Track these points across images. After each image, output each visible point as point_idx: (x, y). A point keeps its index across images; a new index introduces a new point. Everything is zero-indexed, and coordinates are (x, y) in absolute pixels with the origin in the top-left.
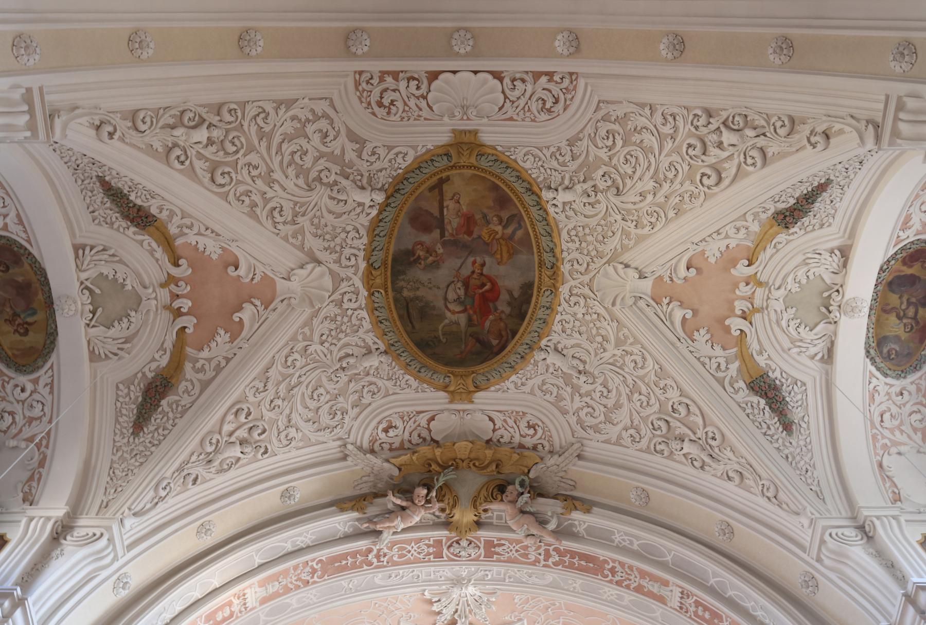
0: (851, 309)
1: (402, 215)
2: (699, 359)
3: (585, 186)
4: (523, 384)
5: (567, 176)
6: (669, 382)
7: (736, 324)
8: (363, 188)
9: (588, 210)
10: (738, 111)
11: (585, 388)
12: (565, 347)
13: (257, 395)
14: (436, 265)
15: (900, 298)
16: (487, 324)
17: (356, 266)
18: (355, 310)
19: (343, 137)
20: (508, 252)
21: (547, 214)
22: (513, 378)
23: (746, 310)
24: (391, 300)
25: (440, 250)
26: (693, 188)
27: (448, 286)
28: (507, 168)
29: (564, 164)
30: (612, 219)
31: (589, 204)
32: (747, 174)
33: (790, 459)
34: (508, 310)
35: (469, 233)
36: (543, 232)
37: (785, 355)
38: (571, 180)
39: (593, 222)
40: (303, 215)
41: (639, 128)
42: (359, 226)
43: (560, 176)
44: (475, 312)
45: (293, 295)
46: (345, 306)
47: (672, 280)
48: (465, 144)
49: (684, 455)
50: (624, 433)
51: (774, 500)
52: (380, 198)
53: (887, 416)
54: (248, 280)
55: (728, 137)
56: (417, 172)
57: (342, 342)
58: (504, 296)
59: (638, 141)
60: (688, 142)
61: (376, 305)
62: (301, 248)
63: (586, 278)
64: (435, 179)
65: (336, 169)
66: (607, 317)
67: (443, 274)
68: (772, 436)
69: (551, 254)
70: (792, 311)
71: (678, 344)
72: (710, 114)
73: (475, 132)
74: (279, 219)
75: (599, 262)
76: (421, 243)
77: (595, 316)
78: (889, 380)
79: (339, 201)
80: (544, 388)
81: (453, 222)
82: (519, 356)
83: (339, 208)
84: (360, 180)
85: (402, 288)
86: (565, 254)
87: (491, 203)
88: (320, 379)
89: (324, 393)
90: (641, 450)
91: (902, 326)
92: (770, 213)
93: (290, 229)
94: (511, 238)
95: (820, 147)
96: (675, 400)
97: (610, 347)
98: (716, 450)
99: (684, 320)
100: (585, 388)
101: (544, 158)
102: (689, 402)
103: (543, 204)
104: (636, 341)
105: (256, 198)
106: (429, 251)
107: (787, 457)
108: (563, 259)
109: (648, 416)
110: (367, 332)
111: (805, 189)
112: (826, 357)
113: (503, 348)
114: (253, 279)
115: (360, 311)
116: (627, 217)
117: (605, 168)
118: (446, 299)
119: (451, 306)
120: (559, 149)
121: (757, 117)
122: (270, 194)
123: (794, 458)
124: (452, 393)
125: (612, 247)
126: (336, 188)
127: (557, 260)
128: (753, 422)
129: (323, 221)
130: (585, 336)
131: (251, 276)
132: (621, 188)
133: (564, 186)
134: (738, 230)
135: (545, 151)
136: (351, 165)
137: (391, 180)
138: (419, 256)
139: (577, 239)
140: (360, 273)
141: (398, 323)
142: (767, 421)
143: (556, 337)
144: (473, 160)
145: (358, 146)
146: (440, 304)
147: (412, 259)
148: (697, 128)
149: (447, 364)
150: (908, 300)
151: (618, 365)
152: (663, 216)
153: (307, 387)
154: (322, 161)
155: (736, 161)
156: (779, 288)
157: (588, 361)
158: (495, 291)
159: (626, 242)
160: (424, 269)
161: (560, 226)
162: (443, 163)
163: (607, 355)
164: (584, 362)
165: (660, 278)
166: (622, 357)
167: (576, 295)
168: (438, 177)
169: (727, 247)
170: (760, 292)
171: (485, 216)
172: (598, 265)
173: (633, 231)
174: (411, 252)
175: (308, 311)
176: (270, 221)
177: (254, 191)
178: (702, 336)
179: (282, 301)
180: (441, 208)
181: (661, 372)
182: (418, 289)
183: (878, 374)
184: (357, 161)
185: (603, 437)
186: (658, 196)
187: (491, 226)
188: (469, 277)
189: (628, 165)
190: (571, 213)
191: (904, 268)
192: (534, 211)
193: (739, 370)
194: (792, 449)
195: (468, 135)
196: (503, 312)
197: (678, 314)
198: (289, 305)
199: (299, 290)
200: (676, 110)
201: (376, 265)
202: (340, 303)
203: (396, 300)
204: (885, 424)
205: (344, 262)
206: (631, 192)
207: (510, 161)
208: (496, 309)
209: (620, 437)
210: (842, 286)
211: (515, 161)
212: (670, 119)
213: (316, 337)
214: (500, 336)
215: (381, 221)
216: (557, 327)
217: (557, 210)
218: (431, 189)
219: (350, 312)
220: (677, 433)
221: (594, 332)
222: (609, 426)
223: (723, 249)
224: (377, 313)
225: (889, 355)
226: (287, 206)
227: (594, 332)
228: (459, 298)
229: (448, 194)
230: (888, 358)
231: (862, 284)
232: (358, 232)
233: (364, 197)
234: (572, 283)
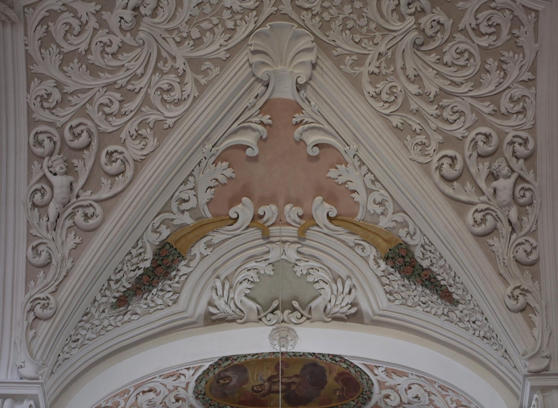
0: (283, 332)
2: (191, 175)
6: (152, 143)
7: (244, 210)
10: (537, 194)
11: (112, 19)
15: (296, 376)
23: (265, 219)
26: (434, 146)
30: (378, 39)
32: (461, 215)
33: (85, 318)
37: (209, 272)
41: (504, 66)
47: (298, 124)
49: (45, 176)
50: (51, 83)
51: (32, 316)
53: (151, 395)
55: (504, 185)
59: (487, 67)
60: (494, 134)
68: (109, 288)
70: (269, 271)
71: (209, 146)
72: (529, 158)
77: (230, 25)
78: (192, 385)
90: (30, 111)
91: (261, 382)
92: (408, 240)
95: (511, 303)
96: (126, 154)
98: (69, 223)
99: (244, 147)
100: (112, 19)
102: (129, 173)
104: (202, 89)
107: (86, 314)
109: (88, 116)
111: (444, 279)
112: (214, 318)
116: (383, 59)
117: (449, 23)
121: (532, 218)
123: (87, 322)
125: (338, 42)
128: (122, 262)
130: (196, 12)
132: (423, 48)
134: (381, 204)
142: (125, 277)
148: (512, 143)
150: (294, 383)
151: (160, 65)
152: (392, 109)
155: (475, 199)
156: (299, 252)
157: (157, 20)
159: (348, 60)
164: (154, 15)
165: (300, 109)
166: (174, 70)
169: (354, 191)
170: (291, 232)
172: (309, 24)
173: (365, 70)
178: (223, 172)
181: (162, 130)
183: (200, 372)
185: (37, 56)
186: (417, 99)
189: (456, 56)
191: (335, 374)
193: (182, 226)
194: (96, 315)
197: (248, 139)
200: (530, 113)
204: (141, 398)
206: (419, 63)
209: (42, 77)
210: (308, 319)
212: (518, 108)
220: (75, 161)
221: (206, 25)
222: (57, 59)
223: (351, 186)
225: (222, 378)
230: (219, 378)
231: (314, 340)
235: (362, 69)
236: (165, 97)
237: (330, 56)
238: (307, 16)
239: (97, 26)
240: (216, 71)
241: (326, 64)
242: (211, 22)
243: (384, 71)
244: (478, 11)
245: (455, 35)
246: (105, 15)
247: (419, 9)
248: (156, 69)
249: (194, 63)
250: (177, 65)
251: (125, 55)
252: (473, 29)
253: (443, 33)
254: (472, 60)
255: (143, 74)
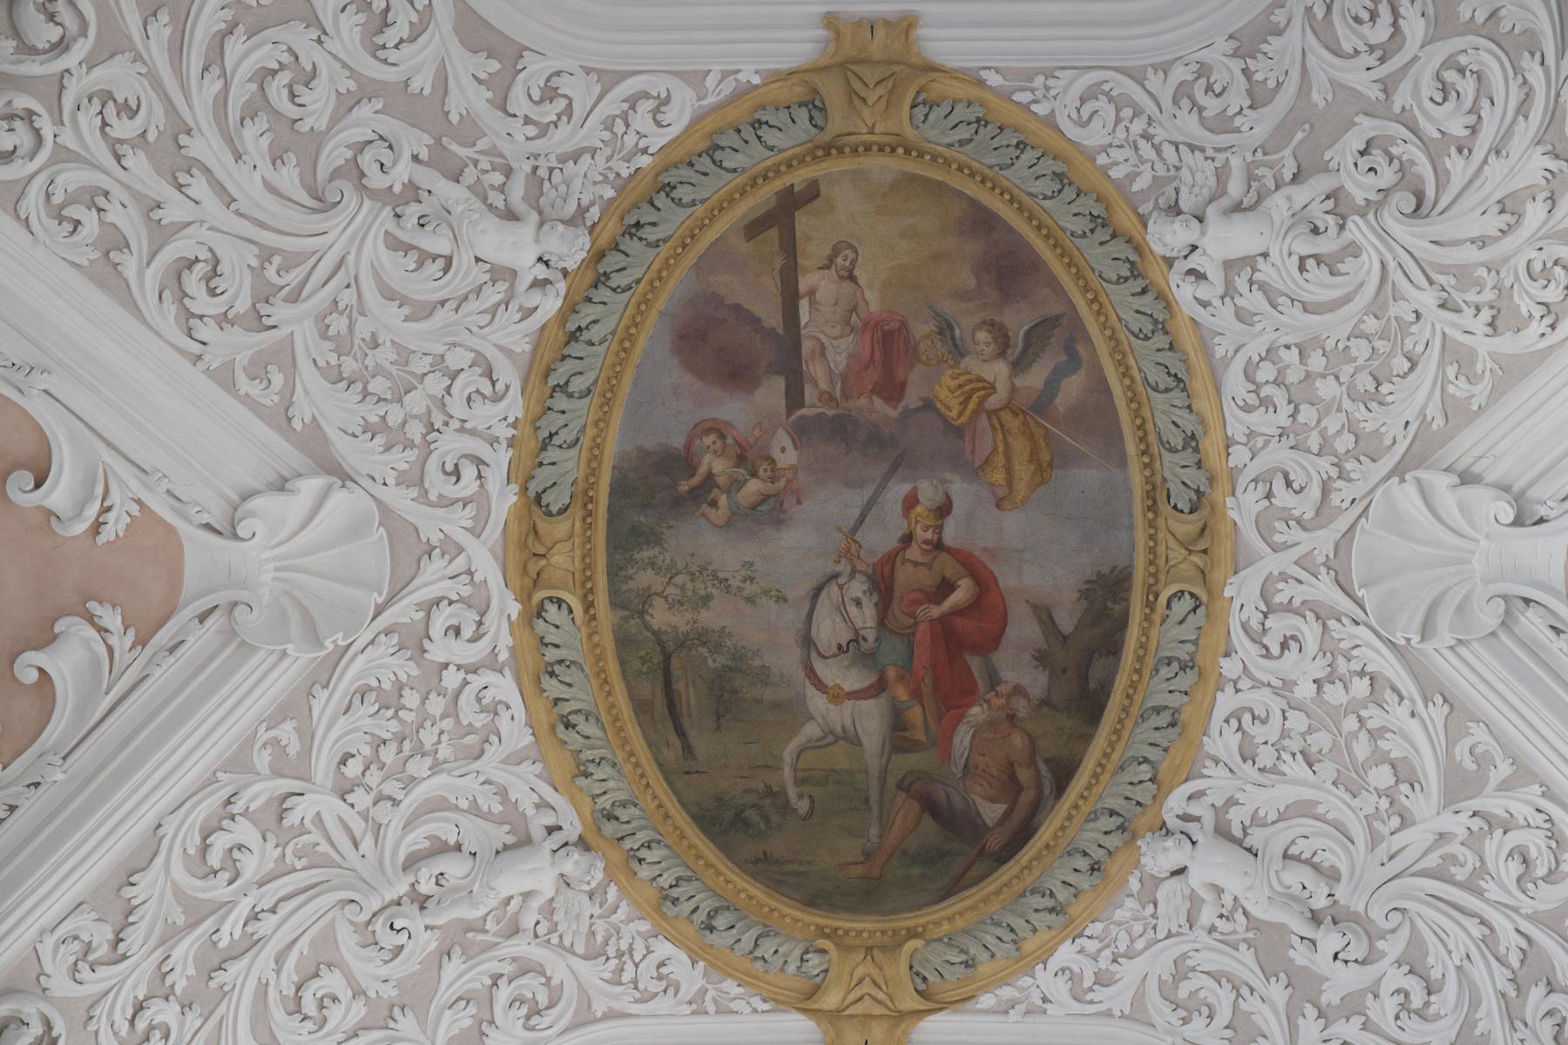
1: (653, 316)
3: (1301, 195)
4: (1103, 980)
5: (1236, 163)
8: (511, 216)
9: (1319, 285)
11: (1341, 982)
12: (1257, 820)
13: (85, 973)
14: (771, 512)
16: (962, 739)
17: (480, 500)
18: (474, 670)
19: (442, 37)
20: (1034, 457)
21: (1168, 307)
22: (1065, 954)
24: (607, 640)
25: (787, 456)
27: (817, 592)
28: (1021, 146)
29: (1222, 124)
30: (1403, 310)
31: (1319, 259)
34: (1036, 682)
35: (892, 390)
36: (1158, 376)
38: (1251, 178)
39: (1335, 327)
40: (295, 298)
42: (491, 353)
43: (1209, 168)
44: (916, 694)
45: (242, 595)
46: (438, 651)
48: (872, 69)
52: (572, 249)
54: (80, 528)
56: (705, 163)
57: (419, 793)
58: (1023, 630)
59: (1480, 17)
61: (551, 655)
62: (281, 418)
63: (1323, 541)
64: (766, 194)
65: (415, 141)
66: (1408, 686)
67: (797, 548)
69: (1188, 457)
73: (906, 25)
74: (201, 303)
75: (1365, 474)
76: (718, 429)
77: (1361, 687)
79: (425, 257)
80: (1184, 991)
81: (831, 350)
82: (1083, 864)
83: (425, 286)
84: (502, 189)
85: (647, 596)
86: (1239, 455)
87: (966, 279)
88: (328, 937)
89: (345, 994)
93: (241, 344)
94: (1042, 404)
97: (1424, 805)
100: (1341, 982)
101: (1151, 108)
103: (1155, 272)
104: (1523, 773)
105: (125, 217)
106: (746, 458)
108: (1233, 473)
110: (515, 759)
113: (1022, 835)
114: (97, 527)
115: (489, 677)
116: (1458, 297)
117: (1367, 127)
118: (807, 642)
119: (829, 672)
120: (1203, 70)
122: (175, 211)
124: (832, 1018)
126: (412, 211)
127: (1211, 480)
129: (363, 328)
131: (93, 510)
132: (1430, 192)
133: (1225, 202)
135: (1154, 81)
136: (469, 131)
137: (609, 193)
138: (710, 476)
139: (1279, 396)
140: (494, 530)
141: (633, 731)
143: (1219, 779)
144: (901, 122)
145: (494, 66)
146: (787, 660)
147: (684, 487)
149: (811, 902)
151: (1460, 874)
153: (280, 960)
154: (365, 111)
158: (988, 604)
159: (1460, 389)
160: (728, 524)
161: (1219, 353)
162: (793, 135)
163: (1416, 838)
164: (1333, 876)
166: (1473, 840)
167: (1288, 608)
168: (778, 185)
171: (946, 328)
172: (1359, 489)
173: (1484, 345)
174: (685, 462)
175: (300, 659)
176: (171, 308)
177: (117, 192)
179: (203, 618)
180: (790, 298)
182: (707, 599)
184: (491, 119)
187: (970, 363)
188: (891, 558)
189: (1450, 105)
190: (1253, 301)
192: (1122, 301)
195: (880, 33)
196: (1018, 690)
198: (231, 633)
199: (267, 576)
201: (555, 500)
202: (415, 642)
203: (624, 642)
205: (437, 484)
206: (1470, 199)
207: (1033, 125)
208: (994, 680)
211: (1050, 122)
213: (323, 766)
214: (1010, 787)
215: (573, 337)
216: (1222, 742)
217: (1203, 292)
218: (754, 228)
219: (452, 679)
221: (1362, 749)
224: (553, 688)
226: (236, 261)
227: (1362, 749)
228: (857, 639)
229: (813, 249)
232: (489, 374)
233: (517, 247)
234: (1272, 564)
235: (1482, 352)
236: (1541, 871)
237: (1448, 436)
238: (1343, 493)
239: (1357, 1021)
240: (1479, 733)
241: (1465, 446)
242: (1354, 735)
243: (1489, 295)
244: (1337, 52)
245: (1397, 109)
246: (1330, 996)
247: (1330, 204)
248: (1469, 887)
249: (1458, 786)
250: (1462, 833)
251: (1431, 960)
252: (1382, 60)
253: (1392, 140)
254: (1463, 60)
255: (1483, 922)
